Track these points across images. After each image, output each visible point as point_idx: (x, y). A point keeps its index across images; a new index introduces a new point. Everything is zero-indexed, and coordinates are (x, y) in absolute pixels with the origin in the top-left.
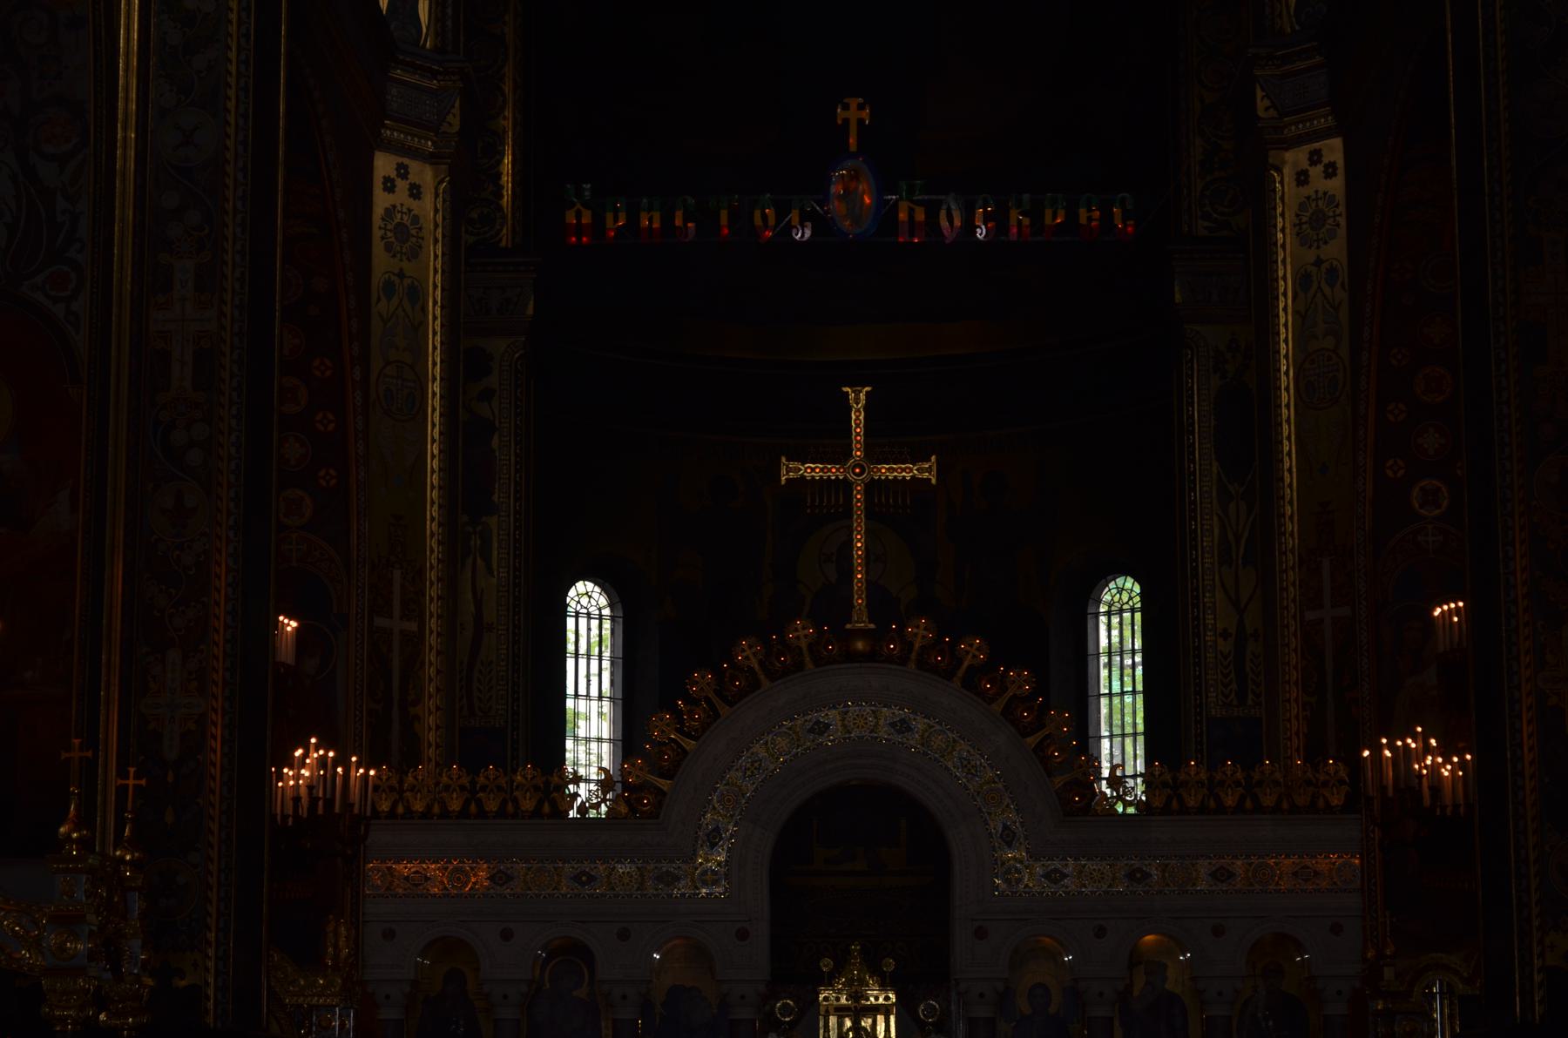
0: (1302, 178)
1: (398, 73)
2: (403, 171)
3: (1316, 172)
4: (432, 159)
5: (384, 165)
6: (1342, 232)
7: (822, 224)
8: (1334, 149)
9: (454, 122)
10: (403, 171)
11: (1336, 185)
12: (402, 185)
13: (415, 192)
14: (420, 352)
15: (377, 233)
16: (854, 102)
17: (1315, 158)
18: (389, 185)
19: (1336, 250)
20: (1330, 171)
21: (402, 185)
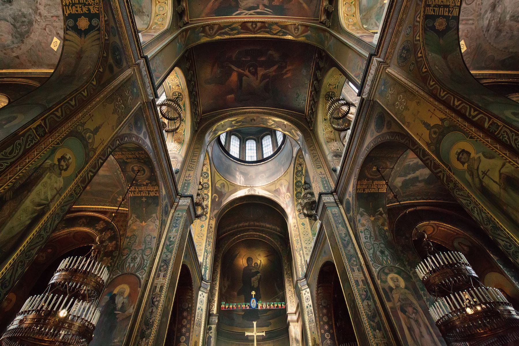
0: (305, 294)
1: (203, 282)
2: (202, 294)
3: (306, 293)
4: (206, 293)
5: (200, 293)
6: (311, 300)
7: (250, 307)
8: (308, 290)
9: (209, 288)
10: (202, 294)
11: (309, 294)
12: (202, 296)
13: (203, 297)
14: (201, 317)
15: (198, 301)
16: (253, 292)
17: (306, 291)
18: (201, 296)
19: (310, 303)
20: (308, 293)
21: (202, 296)
